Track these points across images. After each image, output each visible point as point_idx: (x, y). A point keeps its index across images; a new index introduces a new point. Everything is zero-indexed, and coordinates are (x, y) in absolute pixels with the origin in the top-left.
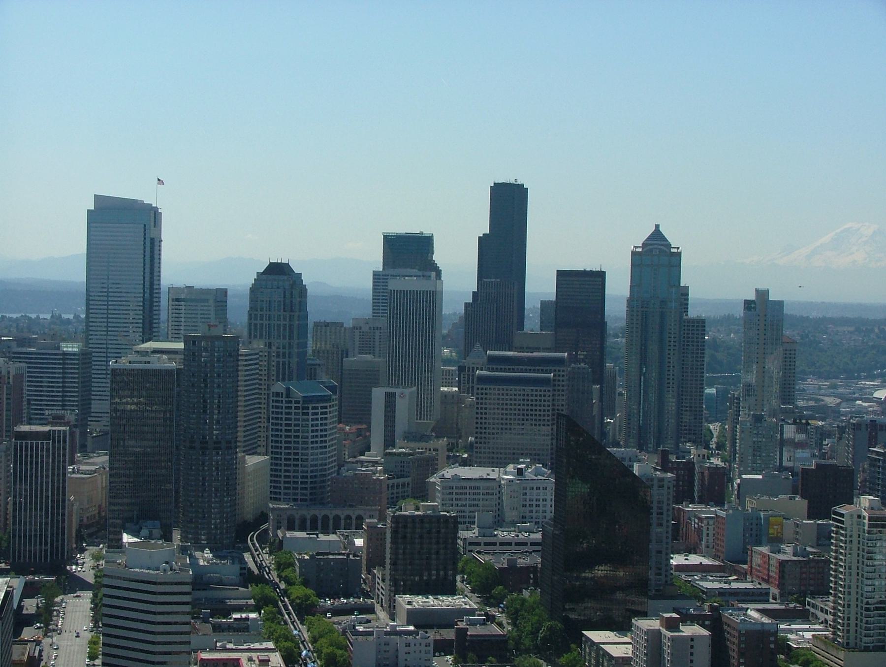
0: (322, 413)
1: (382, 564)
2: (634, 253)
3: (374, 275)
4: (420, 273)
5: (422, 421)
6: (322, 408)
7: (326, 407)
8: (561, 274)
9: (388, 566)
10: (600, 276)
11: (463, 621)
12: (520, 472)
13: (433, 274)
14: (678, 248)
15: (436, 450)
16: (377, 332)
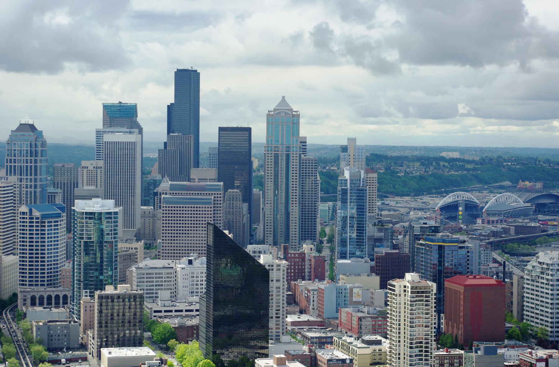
0: (55, 226)
1: (92, 327)
2: (268, 115)
3: (97, 132)
4: (128, 130)
5: (128, 229)
6: (55, 222)
7: (57, 222)
8: (221, 129)
9: (96, 329)
10: (249, 130)
11: (145, 364)
12: (190, 262)
13: (137, 130)
14: (297, 112)
15: (136, 249)
16: (99, 170)
